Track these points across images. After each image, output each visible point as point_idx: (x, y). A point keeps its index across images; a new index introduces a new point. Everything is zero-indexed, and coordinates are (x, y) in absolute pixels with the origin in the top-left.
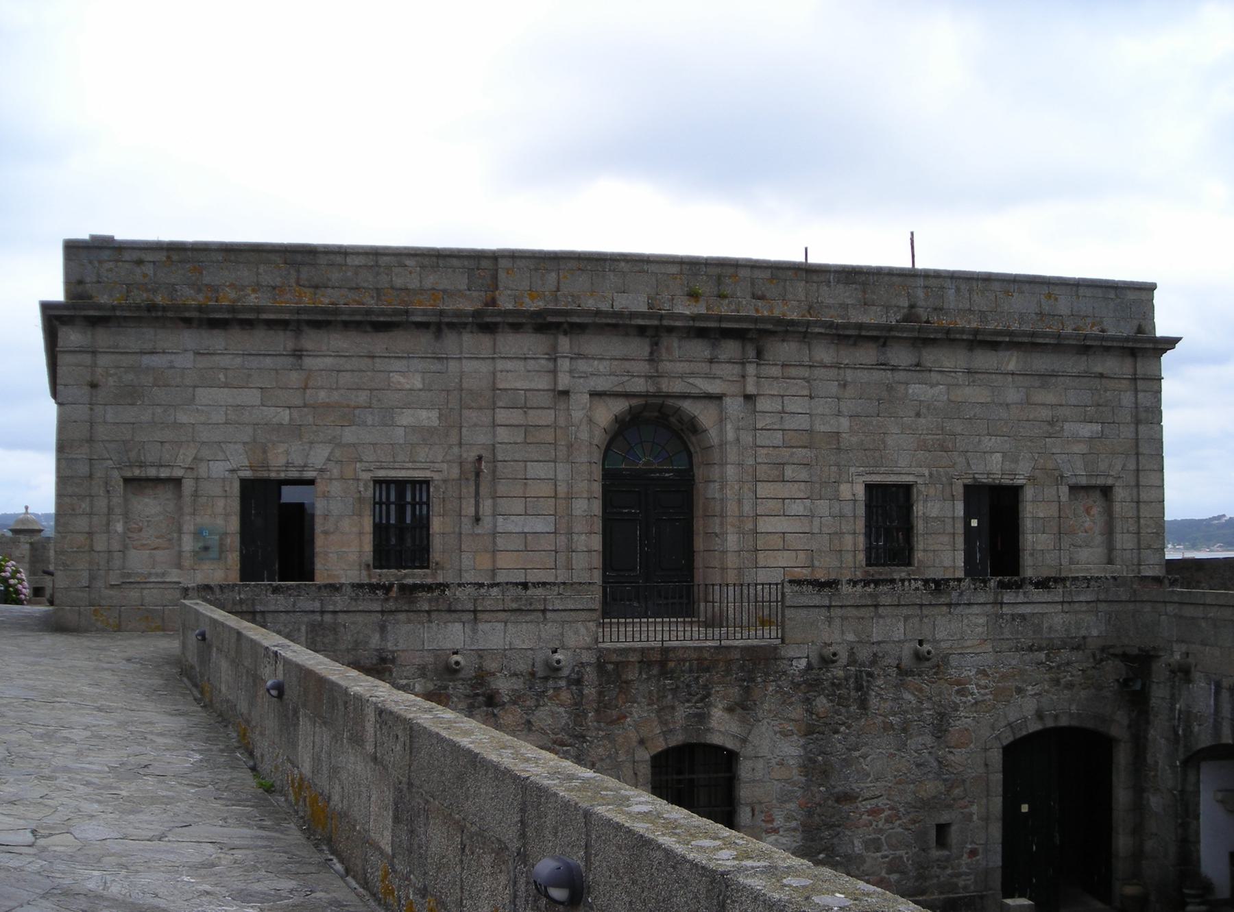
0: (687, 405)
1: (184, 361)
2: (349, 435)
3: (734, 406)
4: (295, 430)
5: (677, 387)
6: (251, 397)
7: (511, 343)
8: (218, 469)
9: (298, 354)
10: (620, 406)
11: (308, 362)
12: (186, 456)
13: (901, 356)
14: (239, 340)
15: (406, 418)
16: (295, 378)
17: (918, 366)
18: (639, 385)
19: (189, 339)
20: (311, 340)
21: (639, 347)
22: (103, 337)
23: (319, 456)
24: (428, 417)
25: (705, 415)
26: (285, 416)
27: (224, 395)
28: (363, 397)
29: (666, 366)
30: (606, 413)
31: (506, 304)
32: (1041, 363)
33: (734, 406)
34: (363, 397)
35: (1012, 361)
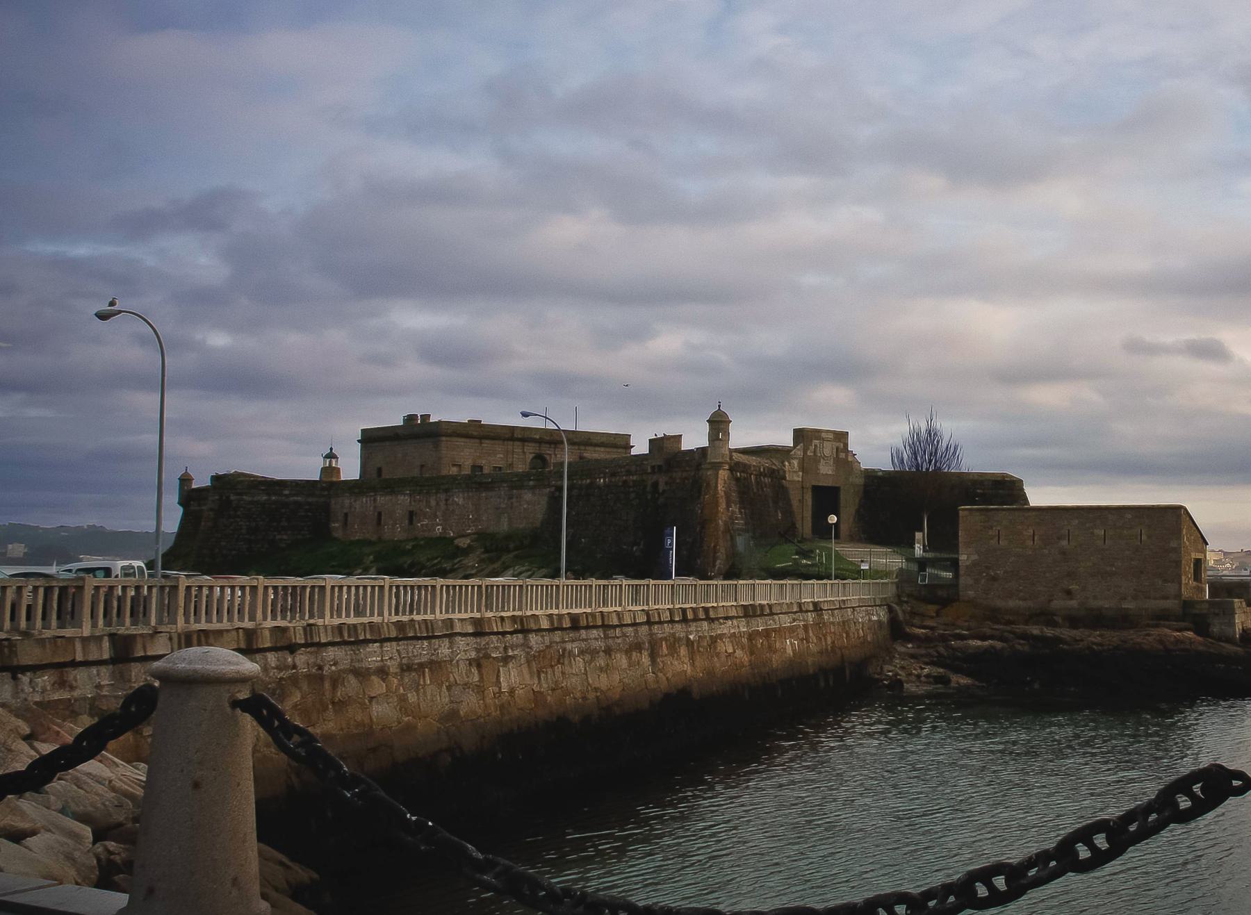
0: (545, 456)
3: (553, 456)
6: (472, 451)
7: (517, 443)
9: (481, 443)
10: (533, 455)
11: (483, 445)
12: (462, 460)
13: (582, 448)
14: (472, 441)
17: (585, 450)
18: (537, 451)
19: (463, 440)
20: (483, 441)
21: (537, 445)
22: (448, 439)
24: (502, 456)
25: (548, 457)
28: (491, 452)
29: (542, 448)
30: (531, 456)
31: (515, 436)
32: (608, 450)
33: (553, 456)
34: (491, 452)
35: (602, 449)
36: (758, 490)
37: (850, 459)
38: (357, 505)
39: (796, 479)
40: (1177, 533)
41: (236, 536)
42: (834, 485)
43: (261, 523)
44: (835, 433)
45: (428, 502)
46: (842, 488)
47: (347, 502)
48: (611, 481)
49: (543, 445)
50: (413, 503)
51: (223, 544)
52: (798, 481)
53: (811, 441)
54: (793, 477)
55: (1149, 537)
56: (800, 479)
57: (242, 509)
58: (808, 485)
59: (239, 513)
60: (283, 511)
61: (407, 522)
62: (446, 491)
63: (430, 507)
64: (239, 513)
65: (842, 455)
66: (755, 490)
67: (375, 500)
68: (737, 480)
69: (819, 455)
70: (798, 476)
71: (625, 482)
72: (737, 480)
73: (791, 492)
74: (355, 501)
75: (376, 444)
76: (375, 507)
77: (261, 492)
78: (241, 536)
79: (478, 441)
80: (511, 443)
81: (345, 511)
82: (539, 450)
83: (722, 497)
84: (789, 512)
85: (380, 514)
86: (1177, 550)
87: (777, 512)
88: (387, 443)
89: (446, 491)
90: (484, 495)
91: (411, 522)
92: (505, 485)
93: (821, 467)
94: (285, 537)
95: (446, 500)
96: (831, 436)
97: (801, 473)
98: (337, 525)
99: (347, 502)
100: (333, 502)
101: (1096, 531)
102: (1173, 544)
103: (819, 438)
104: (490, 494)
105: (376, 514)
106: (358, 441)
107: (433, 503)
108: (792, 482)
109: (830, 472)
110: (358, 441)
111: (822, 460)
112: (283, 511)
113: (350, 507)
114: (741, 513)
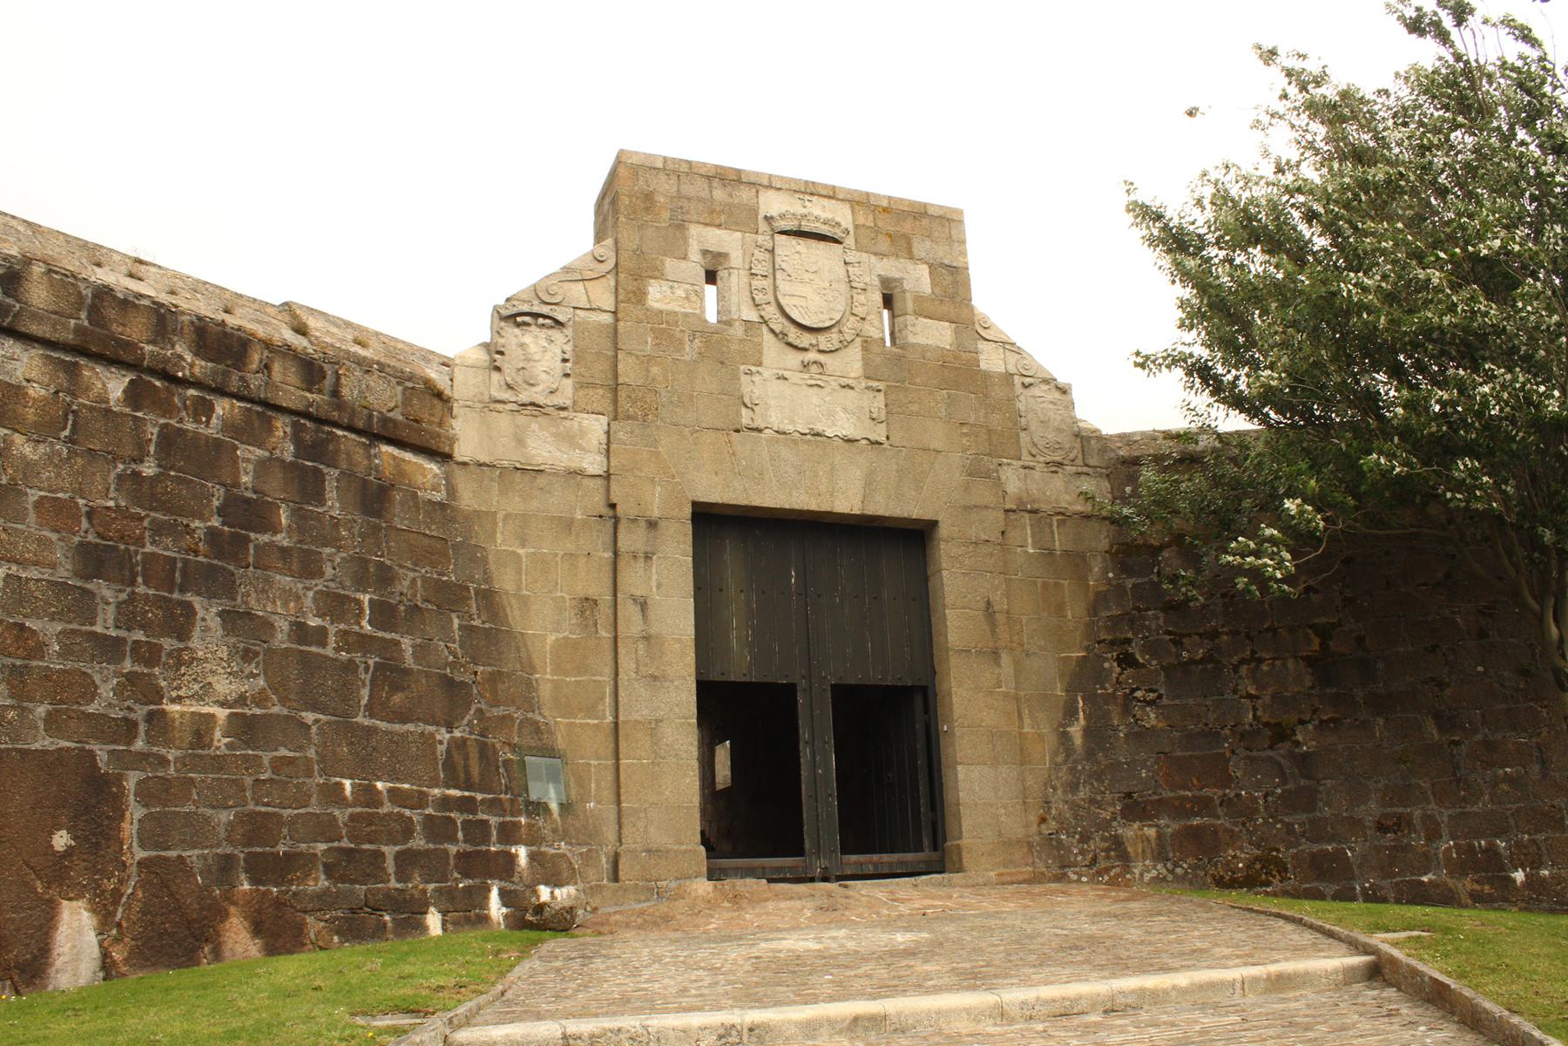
37: (991, 361)
39: (543, 448)
42: (883, 506)
44: (859, 201)
46: (944, 531)
52: (575, 474)
53: (680, 226)
54: (520, 442)
65: (933, 335)
69: (751, 315)
70: (571, 440)
73: (502, 541)
96: (819, 213)
97: (595, 427)
103: (743, 218)
109: (844, 426)
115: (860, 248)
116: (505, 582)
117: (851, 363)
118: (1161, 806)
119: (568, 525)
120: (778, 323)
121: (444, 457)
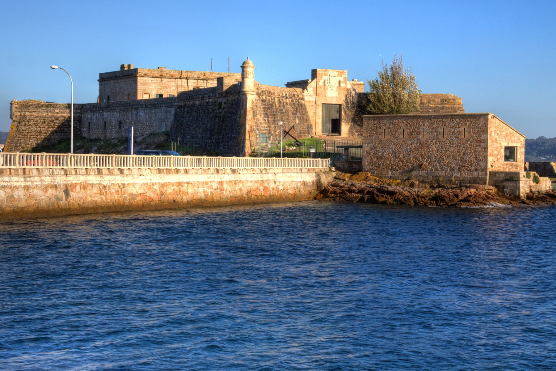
1: (150, 81)
2: (166, 90)
4: (161, 89)
5: (200, 86)
6: (157, 85)
8: (153, 93)
12: (150, 91)
15: (172, 88)
16: (161, 84)
18: (196, 85)
20: (163, 79)
21: (196, 81)
23: (164, 92)
24: (174, 88)
26: (160, 88)
27: (154, 85)
36: (280, 106)
38: (94, 118)
39: (311, 99)
40: (485, 130)
41: (29, 136)
43: (43, 128)
45: (127, 116)
47: (89, 116)
48: (202, 102)
49: (199, 81)
50: (120, 116)
51: (22, 141)
52: (313, 101)
53: (322, 76)
55: (469, 132)
56: (314, 100)
57: (32, 121)
58: (319, 103)
59: (31, 123)
60: (55, 121)
61: (118, 127)
62: (136, 109)
63: (129, 119)
64: (31, 123)
66: (278, 107)
67: (103, 115)
68: (263, 101)
71: (207, 103)
72: (263, 101)
73: (308, 107)
74: (93, 116)
75: (106, 82)
76: (103, 119)
77: (42, 111)
78: (32, 136)
79: (159, 79)
80: (180, 80)
81: (89, 121)
82: (197, 84)
83: (249, 111)
84: (305, 118)
85: (105, 122)
86: (485, 141)
87: (295, 120)
88: (112, 81)
89: (136, 109)
90: (153, 111)
91: (120, 128)
92: (164, 105)
93: (327, 92)
94: (56, 137)
95: (136, 115)
98: (85, 130)
99: (89, 116)
100: (83, 116)
101: (439, 130)
102: (483, 137)
104: (157, 110)
105: (103, 123)
106: (98, 80)
107: (130, 116)
108: (309, 102)
110: (98, 80)
111: (329, 88)
112: (55, 121)
113: (91, 119)
114: (265, 120)
115: (337, 76)
116: (308, 110)
117: (335, 89)
118: (359, 131)
119: (312, 106)
120: (330, 85)
121: (304, 100)
